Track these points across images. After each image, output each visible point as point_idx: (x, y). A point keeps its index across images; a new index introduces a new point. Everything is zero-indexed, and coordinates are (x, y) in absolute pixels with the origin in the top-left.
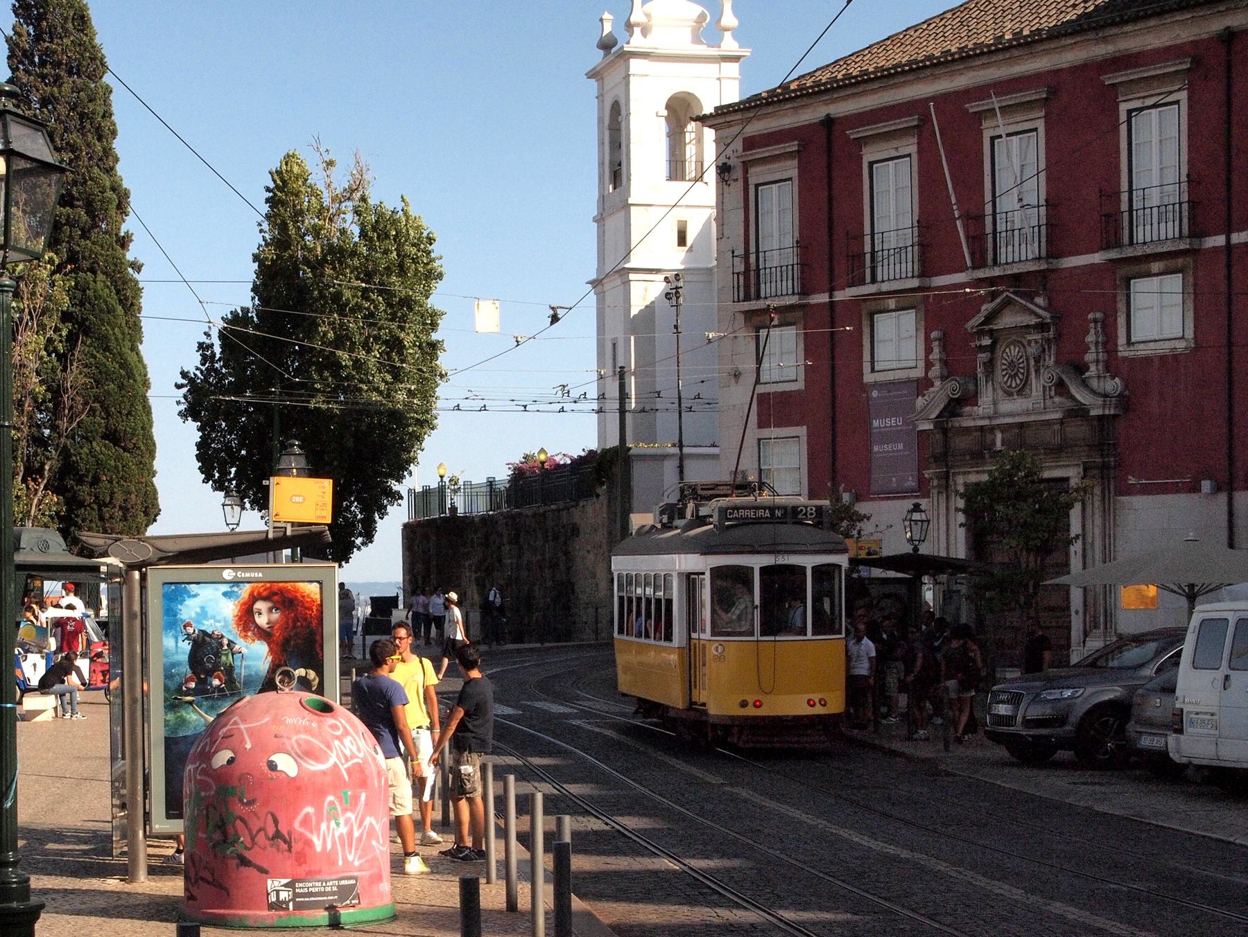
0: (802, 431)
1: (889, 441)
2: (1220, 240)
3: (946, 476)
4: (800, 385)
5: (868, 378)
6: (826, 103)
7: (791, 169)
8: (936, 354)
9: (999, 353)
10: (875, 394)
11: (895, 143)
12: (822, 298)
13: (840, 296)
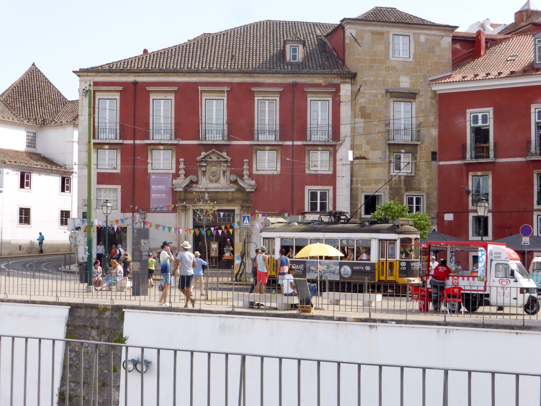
0: (119, 187)
1: (158, 192)
2: (290, 143)
4: (118, 171)
5: (150, 171)
6: (135, 76)
7: (117, 96)
8: (182, 166)
9: (208, 167)
10: (153, 177)
11: (165, 94)
12: (131, 142)
13: (138, 142)
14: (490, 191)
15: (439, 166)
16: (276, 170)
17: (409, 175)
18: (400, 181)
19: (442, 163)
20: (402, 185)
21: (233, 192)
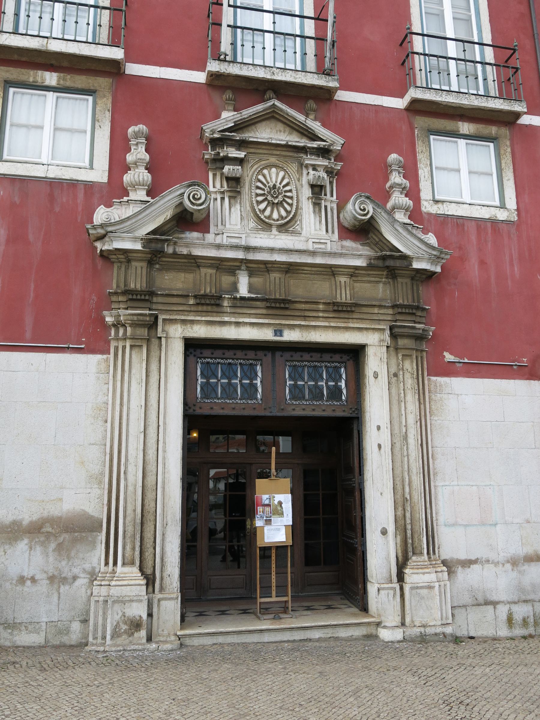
3: (153, 325)
8: (138, 153)
16: (503, 206)
21: (354, 272)
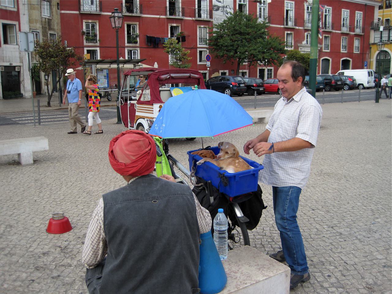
14: (98, 33)
15: (61, 14)
17: (49, 18)
18: (46, 22)
19: (63, 12)
20: (47, 26)
